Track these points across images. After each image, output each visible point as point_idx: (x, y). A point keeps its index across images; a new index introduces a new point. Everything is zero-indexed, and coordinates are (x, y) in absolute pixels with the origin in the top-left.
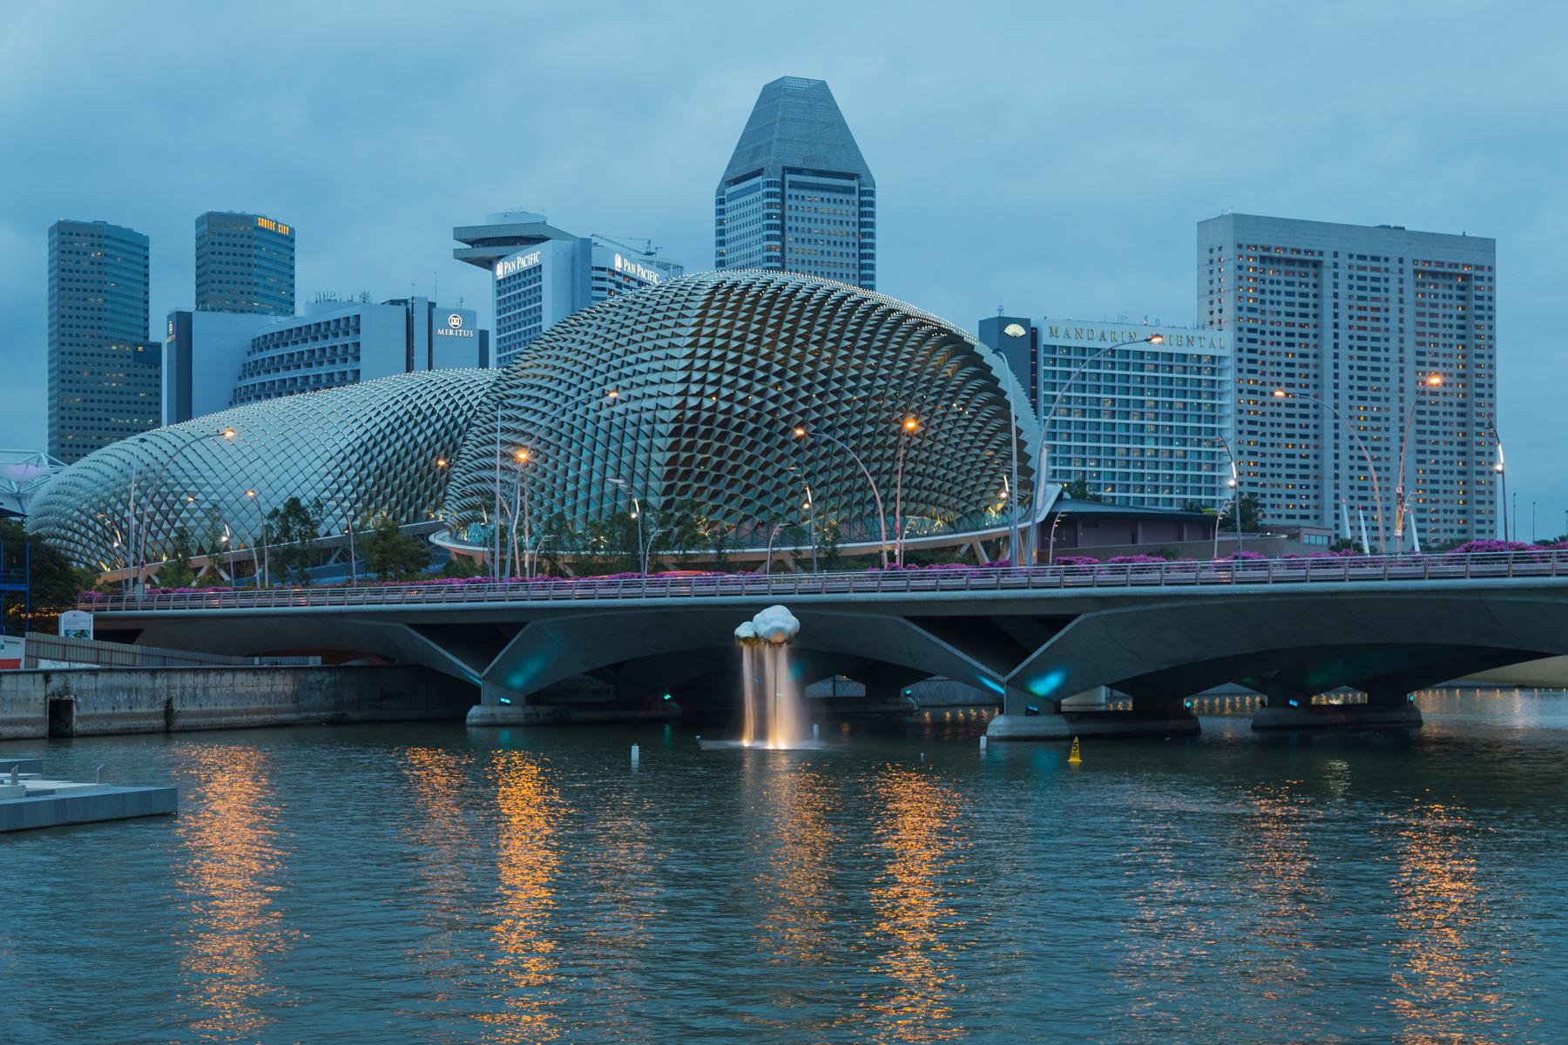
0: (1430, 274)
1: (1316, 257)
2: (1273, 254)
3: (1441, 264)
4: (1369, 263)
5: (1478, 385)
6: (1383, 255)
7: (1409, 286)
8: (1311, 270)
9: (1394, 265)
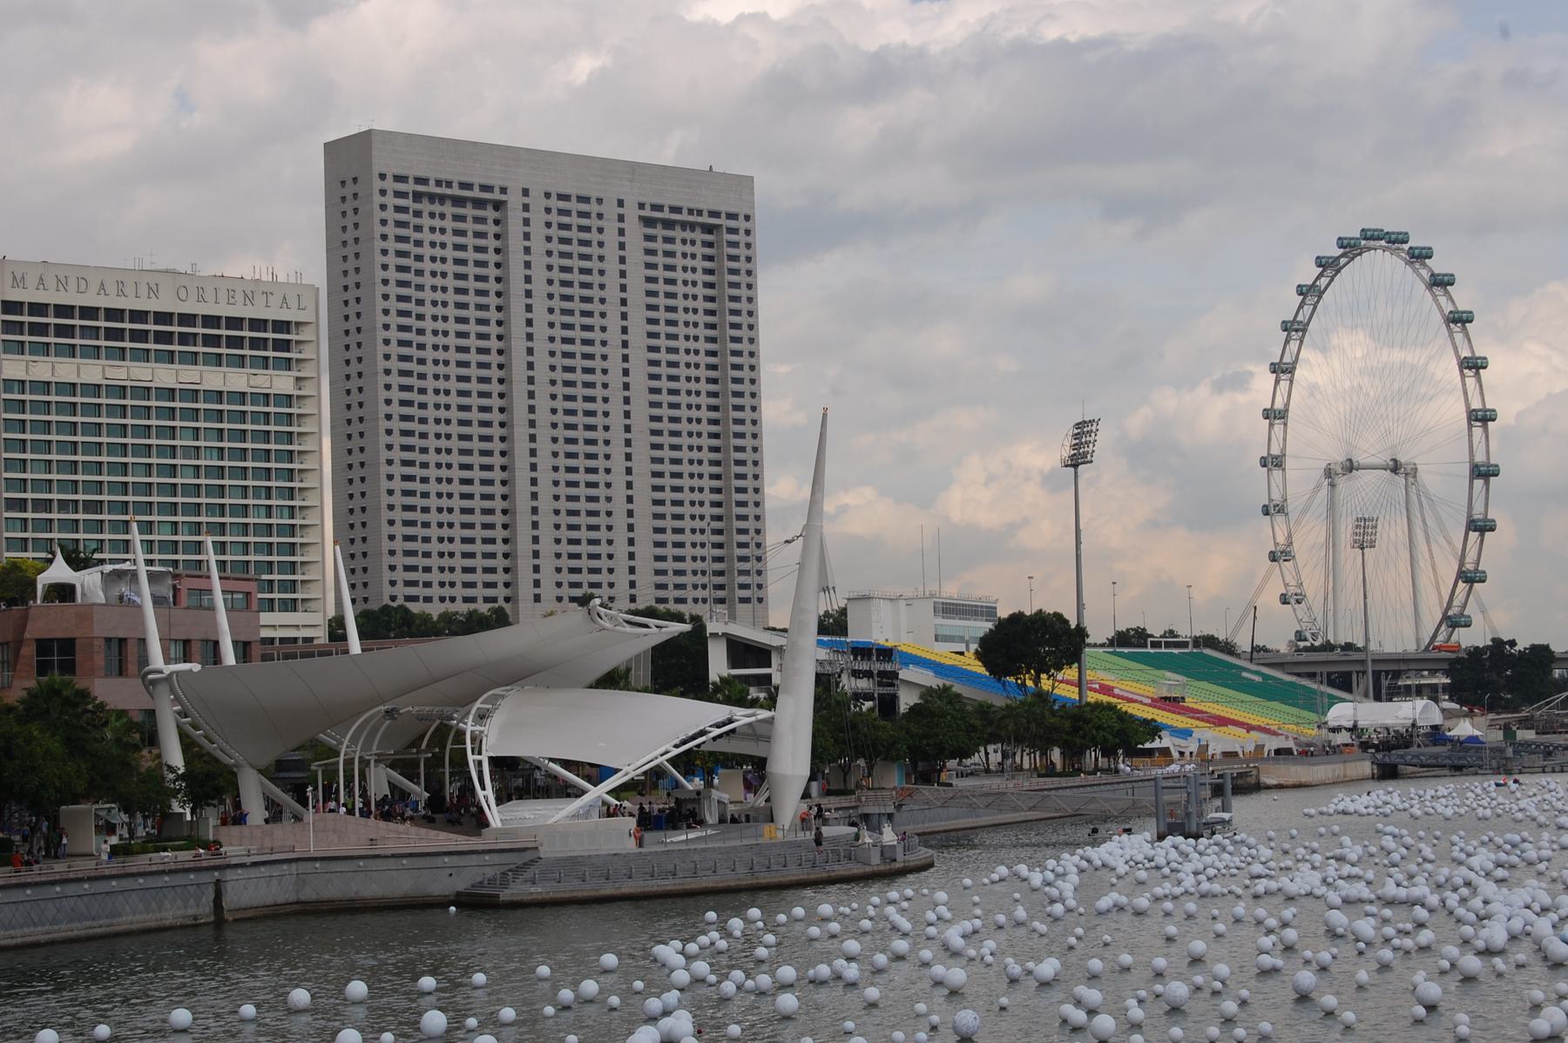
0: (660, 221)
1: (497, 196)
2: (432, 188)
3: (676, 210)
4: (573, 205)
5: (736, 381)
6: (594, 195)
7: (635, 232)
8: (490, 214)
9: (611, 211)
